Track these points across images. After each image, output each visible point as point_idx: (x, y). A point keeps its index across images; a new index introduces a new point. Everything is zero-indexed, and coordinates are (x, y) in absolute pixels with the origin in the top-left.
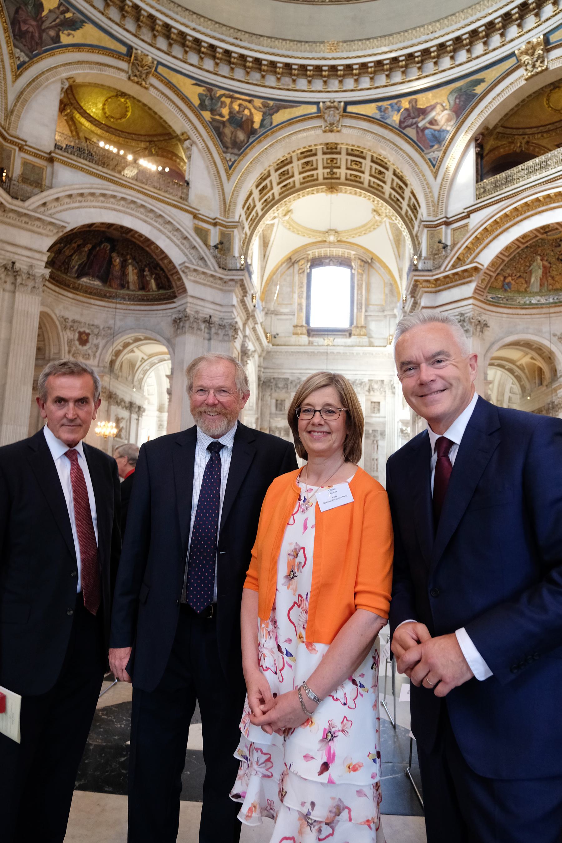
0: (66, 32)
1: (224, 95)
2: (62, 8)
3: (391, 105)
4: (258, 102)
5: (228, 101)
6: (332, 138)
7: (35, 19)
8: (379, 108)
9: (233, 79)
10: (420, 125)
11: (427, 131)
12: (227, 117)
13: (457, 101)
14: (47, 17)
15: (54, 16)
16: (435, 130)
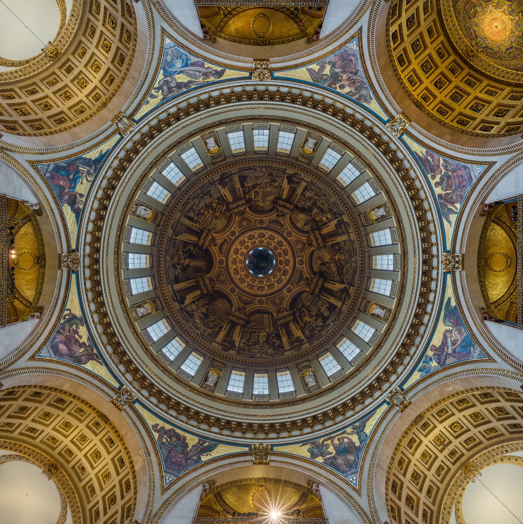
0: (205, 454)
1: (325, 440)
2: (201, 443)
3: (423, 363)
4: (349, 430)
5: (329, 442)
6: (412, 413)
7: (183, 454)
8: (420, 370)
9: (326, 428)
10: (450, 352)
11: (457, 350)
12: (334, 452)
13: (451, 320)
14: (191, 450)
15: (196, 448)
16: (460, 344)
